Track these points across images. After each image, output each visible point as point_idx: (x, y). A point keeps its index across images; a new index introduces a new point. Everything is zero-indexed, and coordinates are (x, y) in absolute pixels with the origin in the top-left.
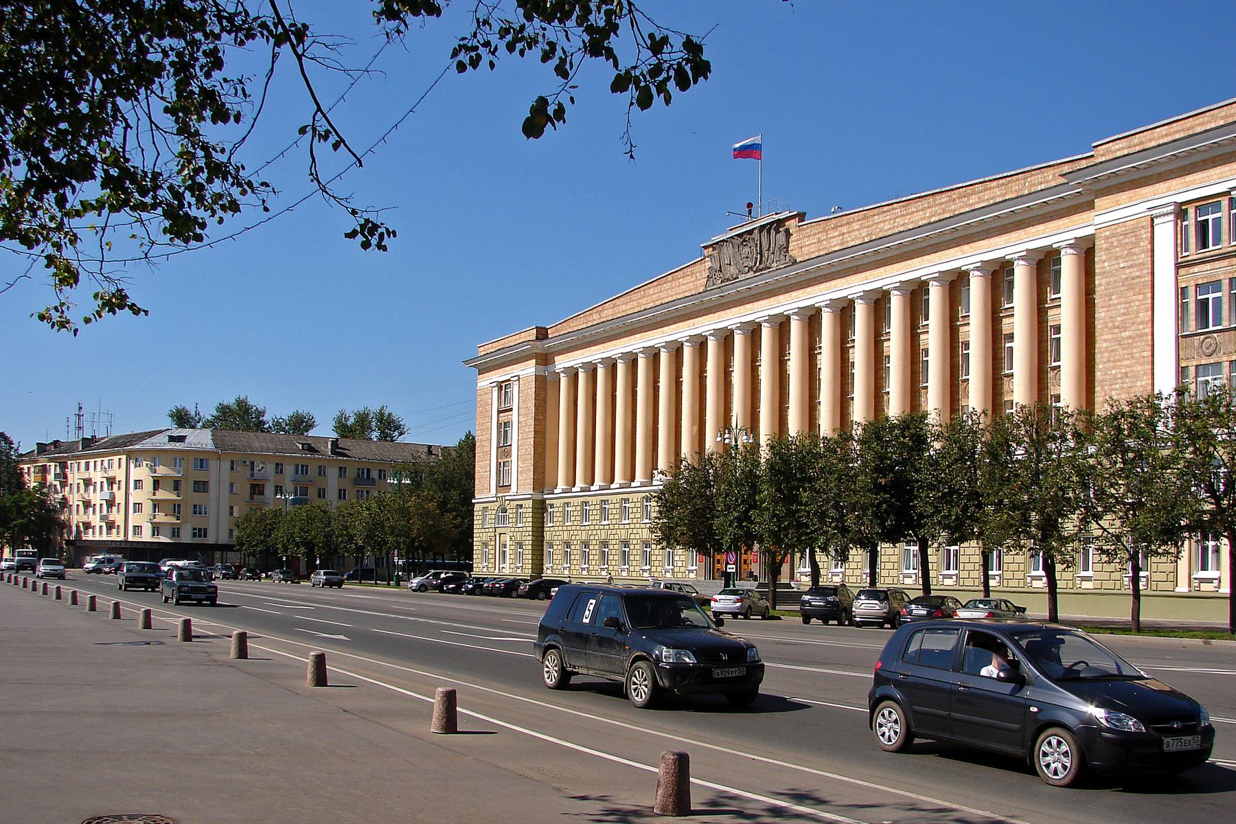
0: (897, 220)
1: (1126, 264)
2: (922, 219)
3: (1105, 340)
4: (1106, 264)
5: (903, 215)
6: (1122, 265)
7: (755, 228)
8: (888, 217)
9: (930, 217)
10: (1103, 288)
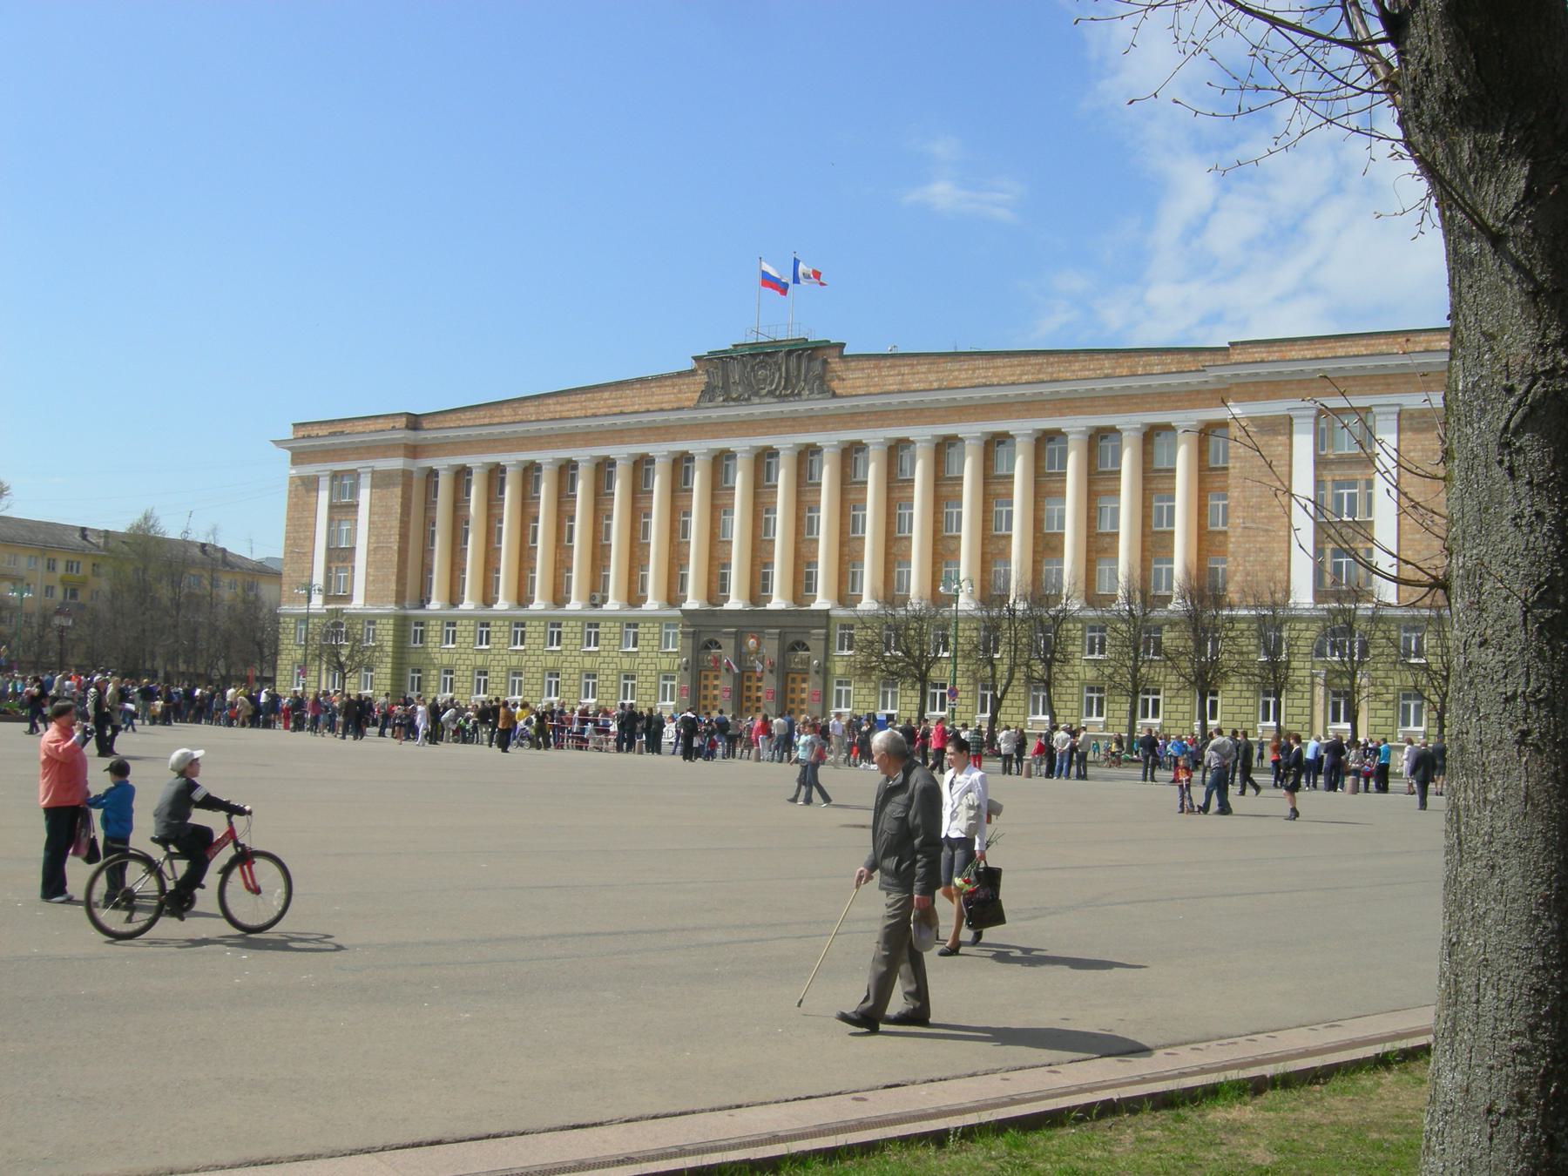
2: (1010, 376)
5: (987, 368)
8: (966, 367)
9: (1021, 375)
10: (1237, 470)
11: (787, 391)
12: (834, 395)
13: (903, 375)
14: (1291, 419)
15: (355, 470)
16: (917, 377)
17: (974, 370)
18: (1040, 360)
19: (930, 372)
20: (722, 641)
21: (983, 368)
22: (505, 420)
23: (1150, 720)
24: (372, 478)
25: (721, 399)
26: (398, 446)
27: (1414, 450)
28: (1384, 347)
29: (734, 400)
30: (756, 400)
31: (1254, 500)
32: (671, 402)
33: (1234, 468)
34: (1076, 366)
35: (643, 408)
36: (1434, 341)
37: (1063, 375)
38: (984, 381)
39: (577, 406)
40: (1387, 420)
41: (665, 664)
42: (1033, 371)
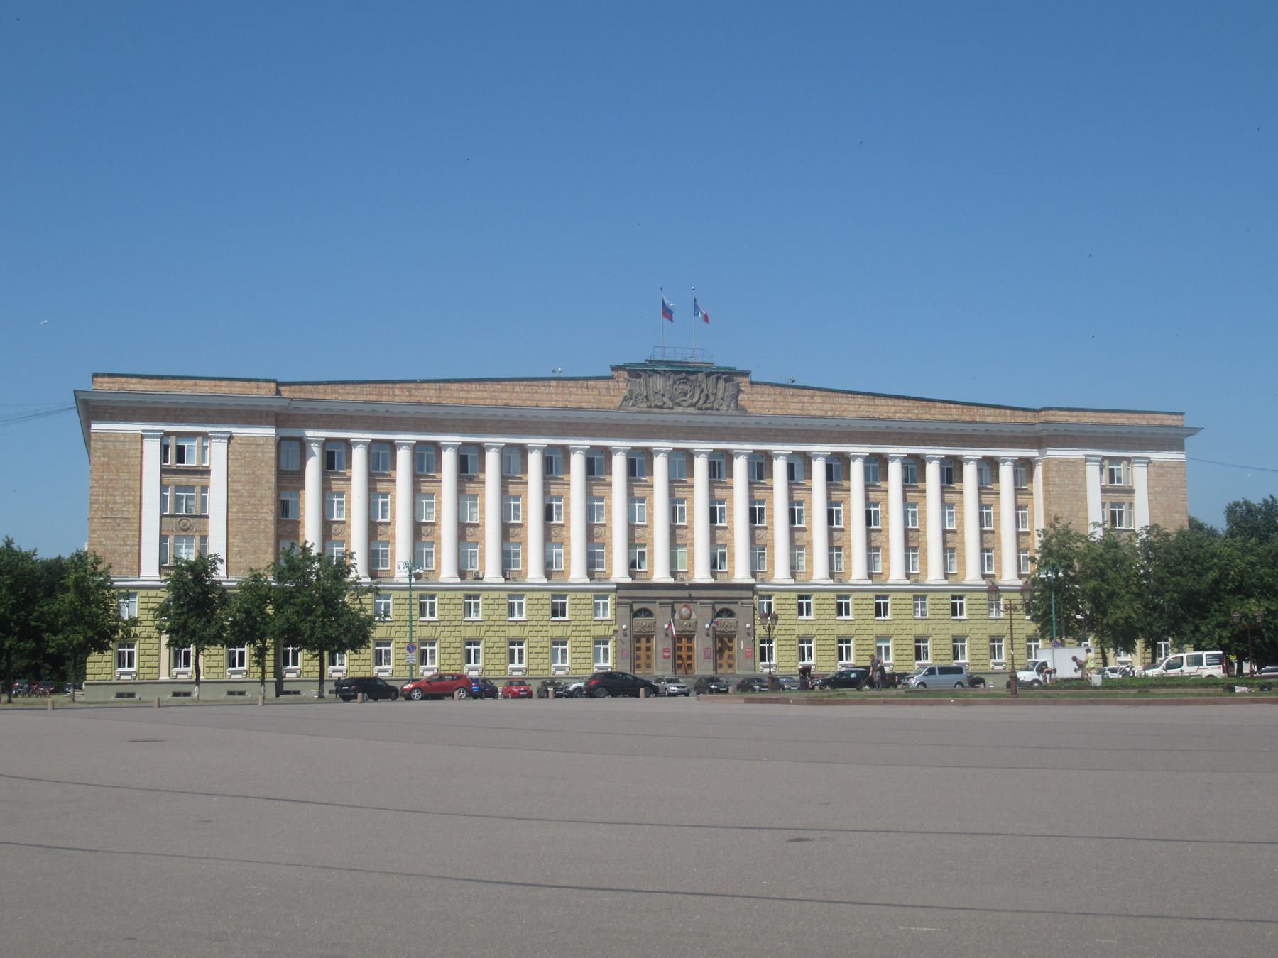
0: (862, 407)
1: (1069, 482)
2: (887, 413)
4: (1056, 480)
5: (868, 405)
6: (1067, 482)
11: (706, 405)
16: (815, 406)
17: (860, 405)
18: (911, 403)
19: (823, 403)
20: (655, 608)
24: (229, 443)
25: (645, 405)
26: (268, 414)
27: (1157, 487)
28: (1138, 420)
30: (680, 409)
31: (1067, 513)
32: (590, 402)
33: (1053, 491)
36: (1164, 419)
39: (485, 394)
41: (600, 631)
42: (903, 411)
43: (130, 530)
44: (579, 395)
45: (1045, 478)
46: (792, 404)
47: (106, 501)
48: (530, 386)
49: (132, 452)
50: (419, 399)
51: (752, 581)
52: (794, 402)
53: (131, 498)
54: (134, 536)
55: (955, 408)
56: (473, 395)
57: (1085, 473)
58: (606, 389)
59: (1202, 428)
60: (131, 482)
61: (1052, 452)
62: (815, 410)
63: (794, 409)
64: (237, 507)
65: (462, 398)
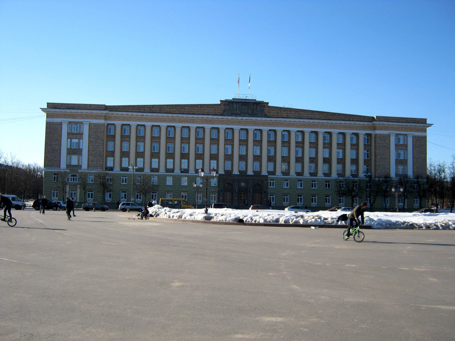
0: (309, 115)
2: (318, 117)
3: (378, 157)
4: (379, 141)
6: (383, 142)
7: (251, 102)
10: (378, 146)
12: (266, 116)
13: (281, 113)
14: (390, 135)
15: (82, 122)
21: (310, 114)
22: (146, 111)
23: (328, 203)
26: (102, 116)
29: (236, 114)
33: (377, 145)
34: (335, 117)
35: (202, 113)
37: (332, 119)
38: (311, 117)
40: (410, 137)
42: (324, 117)
43: (57, 153)
44: (208, 110)
45: (375, 141)
46: (284, 114)
47: (50, 144)
48: (191, 107)
49: (58, 128)
50: (153, 111)
51: (267, 174)
52: (284, 113)
53: (58, 143)
54: (58, 155)
55: (343, 116)
56: (172, 110)
57: (390, 139)
58: (217, 108)
59: (433, 124)
60: (58, 138)
61: (378, 132)
62: (292, 116)
63: (284, 116)
64: (91, 146)
65: (168, 111)
